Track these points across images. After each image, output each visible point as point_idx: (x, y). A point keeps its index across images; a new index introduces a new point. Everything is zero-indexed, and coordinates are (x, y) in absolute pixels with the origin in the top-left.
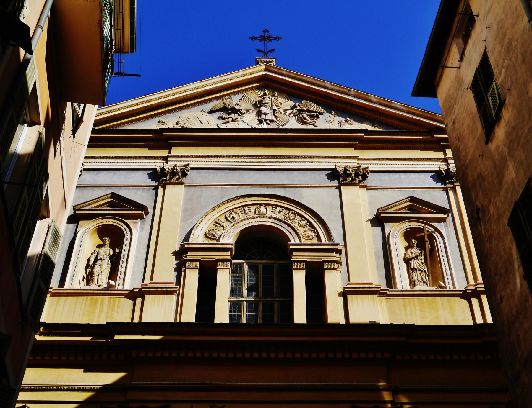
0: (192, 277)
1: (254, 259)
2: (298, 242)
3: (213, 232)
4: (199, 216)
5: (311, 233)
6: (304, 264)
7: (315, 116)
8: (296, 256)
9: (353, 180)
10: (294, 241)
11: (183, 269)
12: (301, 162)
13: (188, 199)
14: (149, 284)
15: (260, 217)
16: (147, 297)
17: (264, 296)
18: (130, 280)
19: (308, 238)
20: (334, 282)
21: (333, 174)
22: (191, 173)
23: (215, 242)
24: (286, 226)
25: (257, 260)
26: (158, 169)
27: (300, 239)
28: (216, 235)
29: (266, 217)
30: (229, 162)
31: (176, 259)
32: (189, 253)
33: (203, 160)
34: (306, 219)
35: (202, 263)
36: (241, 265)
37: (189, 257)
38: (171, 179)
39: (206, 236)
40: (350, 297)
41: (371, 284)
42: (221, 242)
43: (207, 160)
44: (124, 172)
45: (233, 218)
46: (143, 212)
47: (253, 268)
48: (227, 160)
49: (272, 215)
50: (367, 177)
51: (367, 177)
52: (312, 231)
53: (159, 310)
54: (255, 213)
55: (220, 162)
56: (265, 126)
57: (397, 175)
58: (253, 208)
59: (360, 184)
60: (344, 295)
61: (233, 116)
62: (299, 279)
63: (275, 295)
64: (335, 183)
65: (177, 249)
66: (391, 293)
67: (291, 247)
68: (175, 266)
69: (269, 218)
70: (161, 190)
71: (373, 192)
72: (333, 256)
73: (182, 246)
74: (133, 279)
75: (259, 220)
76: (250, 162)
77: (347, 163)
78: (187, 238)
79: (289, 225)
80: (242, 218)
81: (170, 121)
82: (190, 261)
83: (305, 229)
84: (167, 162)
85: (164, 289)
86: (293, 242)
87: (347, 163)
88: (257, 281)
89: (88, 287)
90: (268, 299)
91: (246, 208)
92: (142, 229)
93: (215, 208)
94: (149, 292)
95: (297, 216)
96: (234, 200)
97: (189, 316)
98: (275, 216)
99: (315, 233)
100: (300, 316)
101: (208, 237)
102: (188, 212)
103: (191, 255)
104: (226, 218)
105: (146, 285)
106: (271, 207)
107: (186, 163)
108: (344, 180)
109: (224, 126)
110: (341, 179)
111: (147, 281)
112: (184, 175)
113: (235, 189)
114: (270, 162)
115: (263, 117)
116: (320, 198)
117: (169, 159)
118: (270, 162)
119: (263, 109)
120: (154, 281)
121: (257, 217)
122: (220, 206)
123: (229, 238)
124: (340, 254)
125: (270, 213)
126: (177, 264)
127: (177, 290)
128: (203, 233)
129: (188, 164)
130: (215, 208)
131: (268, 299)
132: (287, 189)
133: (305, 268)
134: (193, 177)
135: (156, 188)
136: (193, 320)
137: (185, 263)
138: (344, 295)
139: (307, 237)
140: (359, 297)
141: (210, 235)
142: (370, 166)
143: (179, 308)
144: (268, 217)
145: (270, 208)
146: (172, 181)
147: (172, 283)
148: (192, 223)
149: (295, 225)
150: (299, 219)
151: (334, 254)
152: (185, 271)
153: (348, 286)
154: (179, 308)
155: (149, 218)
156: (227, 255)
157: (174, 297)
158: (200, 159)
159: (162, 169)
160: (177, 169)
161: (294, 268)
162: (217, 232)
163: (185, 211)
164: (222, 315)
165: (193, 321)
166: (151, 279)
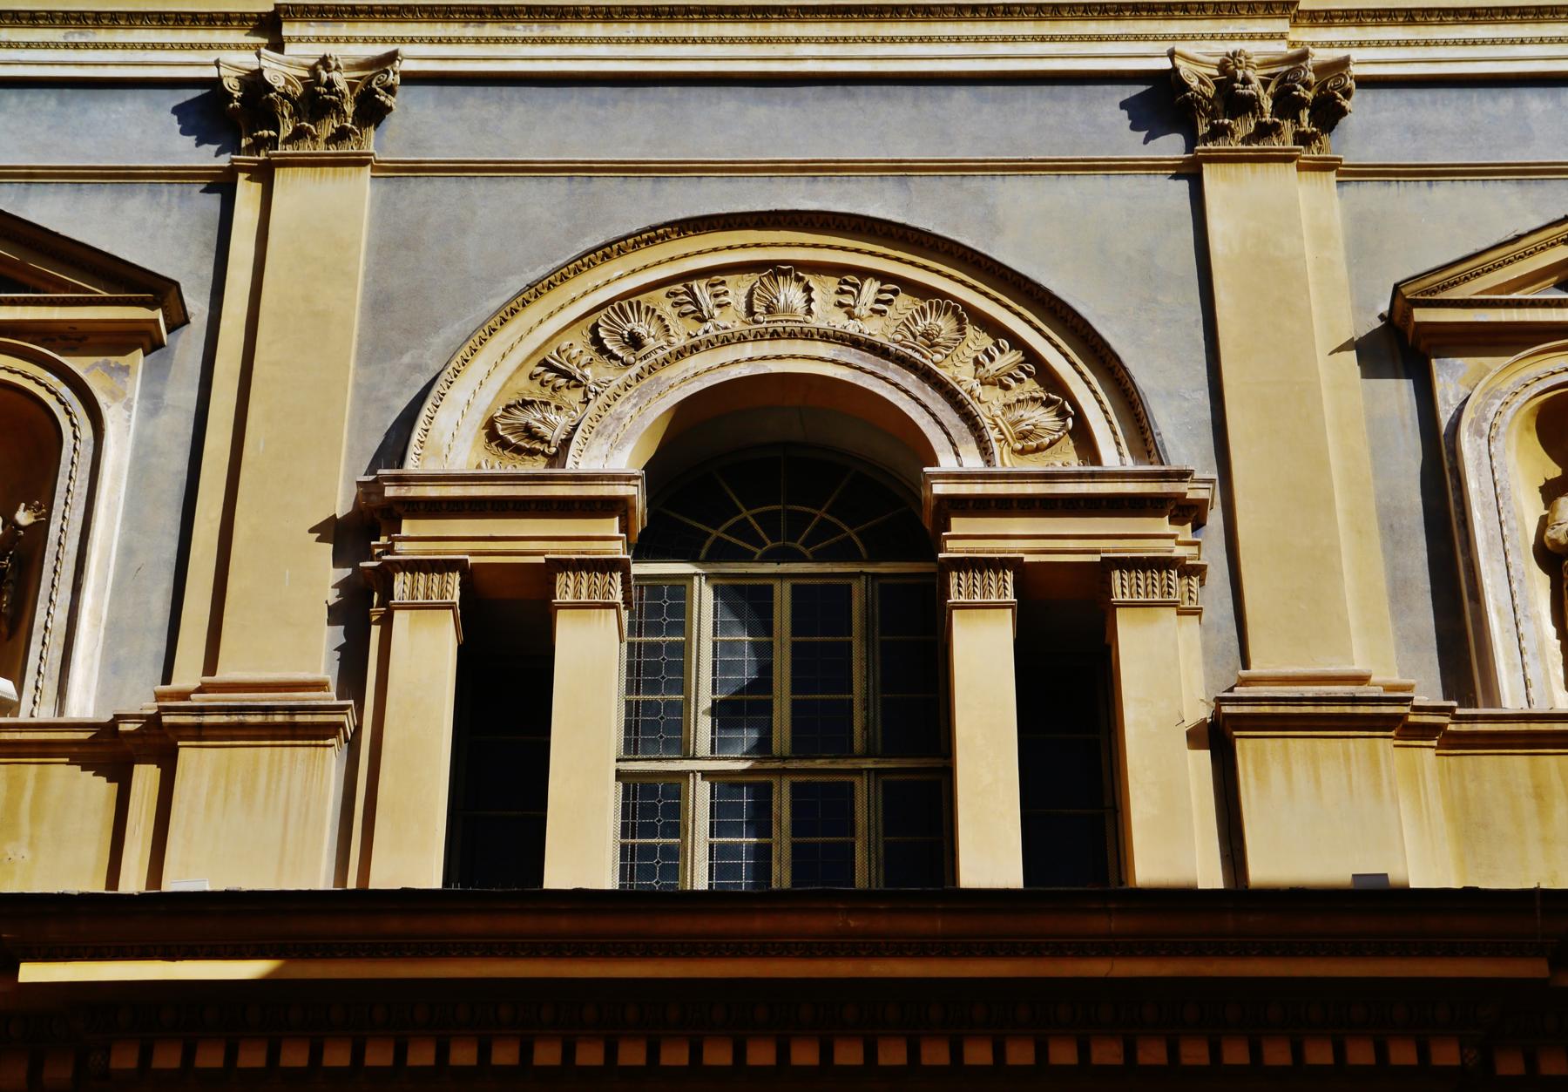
0: (425, 656)
1: (747, 557)
2: (972, 461)
3: (532, 417)
4: (452, 331)
5: (1044, 418)
6: (1010, 577)
8: (965, 537)
9: (1264, 131)
10: (954, 462)
11: (376, 612)
12: (987, 39)
14: (200, 690)
15: (775, 335)
16: (190, 757)
17: (803, 745)
19: (1027, 442)
20: (1162, 672)
21: (1160, 101)
22: (406, 107)
23: (538, 466)
24: (910, 381)
25: (766, 558)
26: (231, 83)
27: (985, 450)
28: (544, 429)
29: (808, 336)
30: (608, 41)
31: (337, 562)
32: (408, 527)
33: (471, 31)
34: (1017, 342)
36: (680, 586)
37: (406, 551)
38: (298, 135)
39: (492, 433)
40: (1248, 750)
41: (1361, 680)
42: (570, 467)
43: (490, 30)
44: (48, 101)
45: (635, 342)
46: (158, 314)
47: (745, 602)
48: (598, 30)
49: (839, 321)
50: (1343, 112)
51: (1343, 112)
52: (1047, 403)
53: (249, 829)
54: (750, 311)
55: (562, 40)
57: (1506, 100)
58: (737, 289)
59: (1305, 154)
60: (1218, 737)
62: (983, 657)
63: (858, 744)
64: (1171, 146)
65: (341, 505)
66: (1465, 727)
67: (939, 489)
68: (332, 596)
69: (825, 337)
70: (247, 193)
71: (1371, 193)
72: (1160, 536)
73: (368, 490)
74: (112, 666)
75: (767, 348)
76: (721, 40)
77: (1232, 37)
78: (395, 445)
79: (928, 376)
80: (680, 341)
82: (414, 567)
83: (1011, 397)
84: (278, 46)
85: (279, 718)
86: (947, 462)
87: (1232, 37)
88: (765, 670)
90: (819, 764)
91: (700, 287)
92: (153, 403)
93: (536, 290)
94: (200, 734)
95: (970, 330)
96: (636, 246)
97: (413, 856)
98: (852, 328)
99: (1062, 414)
100: (990, 848)
101: (504, 444)
102: (392, 314)
103: (416, 538)
104: (597, 341)
105: (185, 695)
106: (832, 283)
107: (380, 50)
108: (1218, 132)
110: (1203, 129)
111: (188, 674)
112: (372, 111)
113: (642, 187)
114: (828, 40)
116: (1092, 232)
117: (288, 30)
118: (828, 40)
120: (224, 674)
121: (759, 337)
122: (564, 279)
123: (615, 447)
124: (1198, 525)
125: (827, 315)
126: (342, 586)
127: (348, 720)
128: (477, 419)
129: (392, 57)
130: (536, 290)
131: (819, 764)
132: (917, 182)
133: (1010, 598)
134: (417, 123)
135: (222, 185)
136: (428, 874)
137: (383, 578)
138: (1218, 737)
139: (1024, 436)
140: (1299, 747)
141: (514, 430)
142: (1356, 54)
143: (358, 815)
144: (822, 333)
145: (826, 289)
146: (306, 148)
147: (319, 686)
148: (417, 368)
149: (960, 373)
150: (978, 341)
151: (1163, 525)
152: (387, 622)
153: (1240, 692)
154: (358, 815)
155: (187, 346)
156: (605, 537)
157: (331, 759)
158: (454, 30)
159: (255, 82)
160: (330, 84)
161: (954, 598)
162: (552, 416)
163: (379, 305)
164: (582, 848)
165: (437, 884)
166: (210, 665)
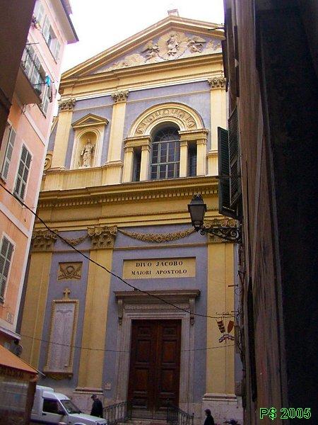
2: (184, 130)
3: (140, 129)
7: (200, 45)
9: (218, 86)
10: (183, 129)
13: (128, 111)
18: (98, 163)
20: (201, 151)
35: (134, 148)
53: (112, 179)
56: (171, 58)
61: (153, 53)
62: (184, 152)
72: (204, 136)
74: (102, 161)
81: (119, 66)
86: (181, 130)
89: (80, 168)
93: (141, 115)
97: (127, 178)
100: (183, 173)
109: (148, 63)
115: (170, 51)
116: (195, 102)
119: (170, 46)
150: (186, 114)
